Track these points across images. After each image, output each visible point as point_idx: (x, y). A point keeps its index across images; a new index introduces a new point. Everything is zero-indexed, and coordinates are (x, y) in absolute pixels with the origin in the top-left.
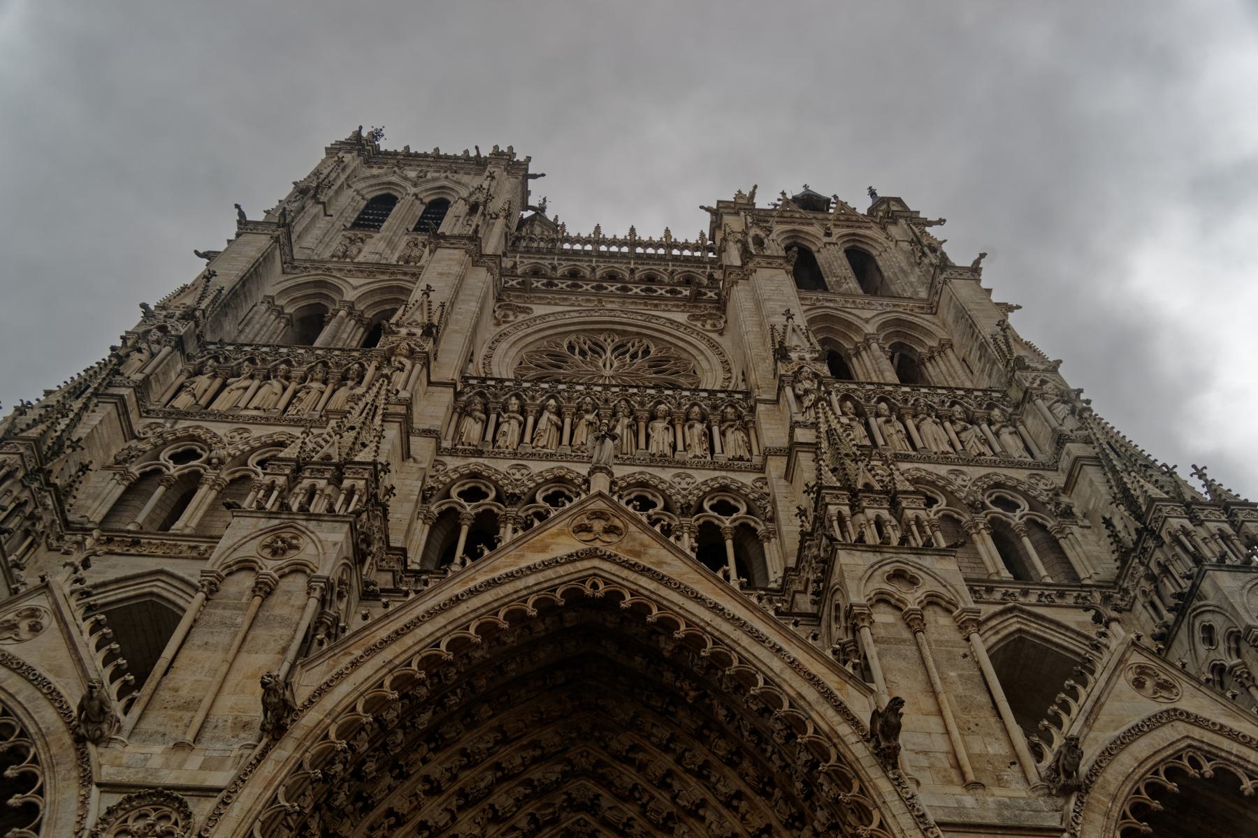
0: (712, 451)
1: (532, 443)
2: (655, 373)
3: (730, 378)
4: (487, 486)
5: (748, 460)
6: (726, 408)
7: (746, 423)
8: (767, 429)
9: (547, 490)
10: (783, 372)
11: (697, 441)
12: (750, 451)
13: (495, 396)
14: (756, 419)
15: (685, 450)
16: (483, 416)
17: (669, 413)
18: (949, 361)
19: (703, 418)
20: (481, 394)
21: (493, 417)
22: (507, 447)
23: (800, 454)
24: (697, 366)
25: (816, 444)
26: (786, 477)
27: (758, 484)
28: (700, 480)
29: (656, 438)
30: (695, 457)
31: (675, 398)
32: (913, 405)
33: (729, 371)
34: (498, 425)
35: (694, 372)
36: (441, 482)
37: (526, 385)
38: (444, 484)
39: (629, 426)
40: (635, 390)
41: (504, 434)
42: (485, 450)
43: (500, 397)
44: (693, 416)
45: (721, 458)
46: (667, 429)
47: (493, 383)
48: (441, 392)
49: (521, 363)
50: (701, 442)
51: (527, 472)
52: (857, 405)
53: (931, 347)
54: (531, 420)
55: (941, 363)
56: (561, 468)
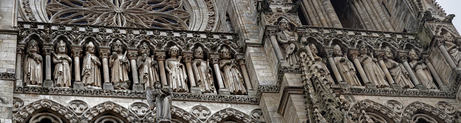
0: (217, 87)
2: (154, 9)
3: (213, 16)
5: (245, 94)
6: (222, 48)
7: (238, 61)
8: (258, 70)
10: (267, 23)
11: (205, 78)
12: (245, 85)
13: (48, 40)
14: (246, 58)
15: (197, 86)
16: (39, 56)
17: (180, 53)
19: (205, 58)
20: (34, 37)
21: (48, 57)
22: (65, 85)
24: (186, 3)
26: (279, 111)
27: (256, 115)
28: (213, 112)
29: (174, 74)
30: (207, 92)
31: (183, 40)
33: (212, 9)
34: (53, 65)
35: (183, 7)
36: (21, 116)
37: (68, 29)
38: (24, 119)
39: (153, 65)
40: (151, 33)
41: (61, 73)
43: (51, 41)
44: (197, 55)
45: (226, 91)
46: (181, 67)
47: (42, 27)
48: (8, 39)
50: (208, 79)
51: (84, 107)
54: (77, 60)
56: (109, 103)
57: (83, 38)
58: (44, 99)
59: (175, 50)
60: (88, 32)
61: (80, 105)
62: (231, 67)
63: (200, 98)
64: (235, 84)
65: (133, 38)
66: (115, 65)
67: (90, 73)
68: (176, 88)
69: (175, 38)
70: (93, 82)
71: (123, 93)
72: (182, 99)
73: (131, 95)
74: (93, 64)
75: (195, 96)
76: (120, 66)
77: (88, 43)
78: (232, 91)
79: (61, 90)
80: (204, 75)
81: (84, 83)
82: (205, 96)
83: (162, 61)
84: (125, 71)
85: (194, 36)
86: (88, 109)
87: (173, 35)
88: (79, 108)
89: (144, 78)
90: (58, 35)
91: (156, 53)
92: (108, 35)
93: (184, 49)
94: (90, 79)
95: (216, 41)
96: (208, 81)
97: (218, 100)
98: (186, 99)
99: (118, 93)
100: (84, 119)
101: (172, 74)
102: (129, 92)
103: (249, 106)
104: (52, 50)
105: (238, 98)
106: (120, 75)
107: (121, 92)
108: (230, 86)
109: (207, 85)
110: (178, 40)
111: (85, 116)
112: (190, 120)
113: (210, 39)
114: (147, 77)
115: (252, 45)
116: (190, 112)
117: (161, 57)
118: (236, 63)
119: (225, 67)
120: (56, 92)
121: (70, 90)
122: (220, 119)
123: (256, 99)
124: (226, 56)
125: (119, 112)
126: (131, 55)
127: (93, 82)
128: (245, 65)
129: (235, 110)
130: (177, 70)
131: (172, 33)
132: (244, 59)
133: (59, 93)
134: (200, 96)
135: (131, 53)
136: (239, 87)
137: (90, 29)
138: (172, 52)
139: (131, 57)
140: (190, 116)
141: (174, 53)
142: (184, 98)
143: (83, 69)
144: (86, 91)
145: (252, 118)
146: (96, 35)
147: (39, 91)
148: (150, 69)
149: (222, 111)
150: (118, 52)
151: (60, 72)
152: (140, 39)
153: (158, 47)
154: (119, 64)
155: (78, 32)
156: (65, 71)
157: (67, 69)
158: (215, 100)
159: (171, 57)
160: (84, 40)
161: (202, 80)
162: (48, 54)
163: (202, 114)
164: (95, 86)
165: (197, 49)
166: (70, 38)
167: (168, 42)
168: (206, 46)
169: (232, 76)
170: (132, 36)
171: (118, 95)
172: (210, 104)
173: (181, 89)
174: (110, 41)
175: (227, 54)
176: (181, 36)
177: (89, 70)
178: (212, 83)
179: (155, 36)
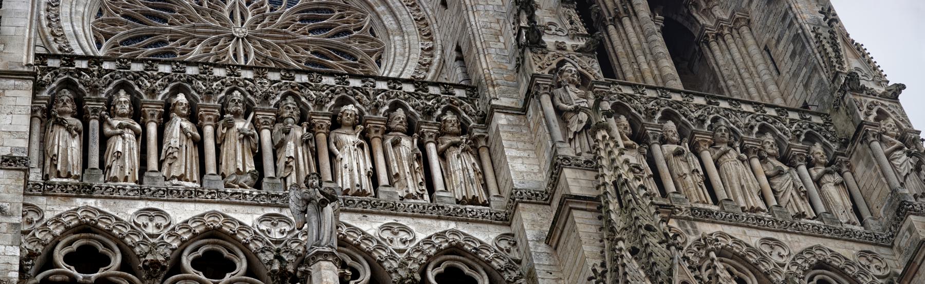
0: (431, 188)
1: (160, 168)
2: (312, 31)
3: (430, 49)
4: (106, 245)
5: (484, 204)
6: (444, 112)
7: (475, 140)
9: (196, 250)
11: (407, 169)
12: (485, 186)
13: (95, 89)
14: (491, 135)
15: (391, 184)
16: (76, 122)
17: (360, 119)
18: (745, 46)
21: (94, 124)
22: (126, 179)
23: (575, 213)
24: (376, 21)
25: (597, 199)
27: (504, 244)
28: (421, 236)
29: (346, 161)
30: (410, 196)
31: (367, 94)
32: (710, 126)
34: (104, 140)
35: (372, 31)
37: (136, 67)
39: (305, 142)
40: (305, 78)
41: (119, 155)
42: (95, 185)
43: (101, 91)
44: (395, 124)
45: (447, 197)
46: (361, 146)
49: (100, 13)
50: (413, 172)
52: (633, 121)
53: (719, 20)
54: (152, 129)
55: (733, 47)
56: (215, 214)
57: (167, 86)
58: (83, 207)
59: (350, 113)
60: (176, 75)
61: (156, 217)
62: (460, 151)
63: (396, 209)
64: (467, 184)
65: (267, 88)
66: (228, 140)
67: (176, 156)
68: (349, 186)
69: (352, 90)
70: (183, 172)
71: (243, 194)
72: (360, 209)
73: (258, 200)
74: (184, 137)
75: (385, 204)
76: (238, 142)
77: (176, 96)
78: (459, 196)
79: (119, 189)
80: (406, 164)
81: (165, 174)
82: (407, 205)
83: (324, 133)
84: (249, 152)
85: (390, 88)
86: (172, 226)
87: (348, 83)
88: (154, 224)
89: (286, 166)
90: (116, 79)
91: (313, 119)
92: (217, 81)
93: (368, 111)
94: (177, 166)
95: (432, 99)
96: (414, 175)
97: (431, 213)
98: (369, 209)
99: (232, 194)
100: (164, 245)
101: (341, 159)
102: (255, 193)
103: (491, 227)
104: (103, 109)
105: (470, 212)
106: (238, 159)
107: (240, 193)
108: (455, 188)
109: (410, 183)
110: (357, 94)
111: (166, 240)
112: (374, 250)
113: (422, 95)
114: (291, 164)
116: (375, 234)
117: (322, 125)
118: (470, 143)
119: (448, 150)
120: (108, 192)
121: (135, 188)
122: (433, 251)
123: (506, 214)
124: (451, 128)
125: (234, 231)
126: (262, 121)
127: (183, 172)
128: (489, 149)
129: (464, 234)
130: (352, 152)
131: (346, 80)
132: (487, 135)
133: (114, 195)
134: (396, 204)
135: (261, 116)
136: (474, 191)
137: (181, 68)
138: (345, 117)
139: (262, 123)
140: (375, 244)
141: (348, 118)
143: (164, 147)
144: (169, 191)
145: (496, 251)
146: (192, 80)
147: (74, 190)
148: (300, 149)
149: (438, 235)
150: (236, 114)
151: (118, 152)
152: (281, 90)
153: (317, 107)
154: (238, 138)
155: (155, 73)
156: (127, 150)
157: (132, 146)
158: (425, 213)
159: (343, 127)
160: (167, 90)
161: (401, 174)
163: (399, 239)
164: (187, 180)
165: (395, 113)
166: (140, 86)
167: (336, 97)
168: (413, 108)
169: (461, 168)
170: (265, 83)
171: (233, 200)
172: (416, 220)
173: (358, 190)
174: (220, 93)
175: (453, 125)
176: (365, 86)
177: (176, 150)
178: (421, 181)
179: (311, 85)
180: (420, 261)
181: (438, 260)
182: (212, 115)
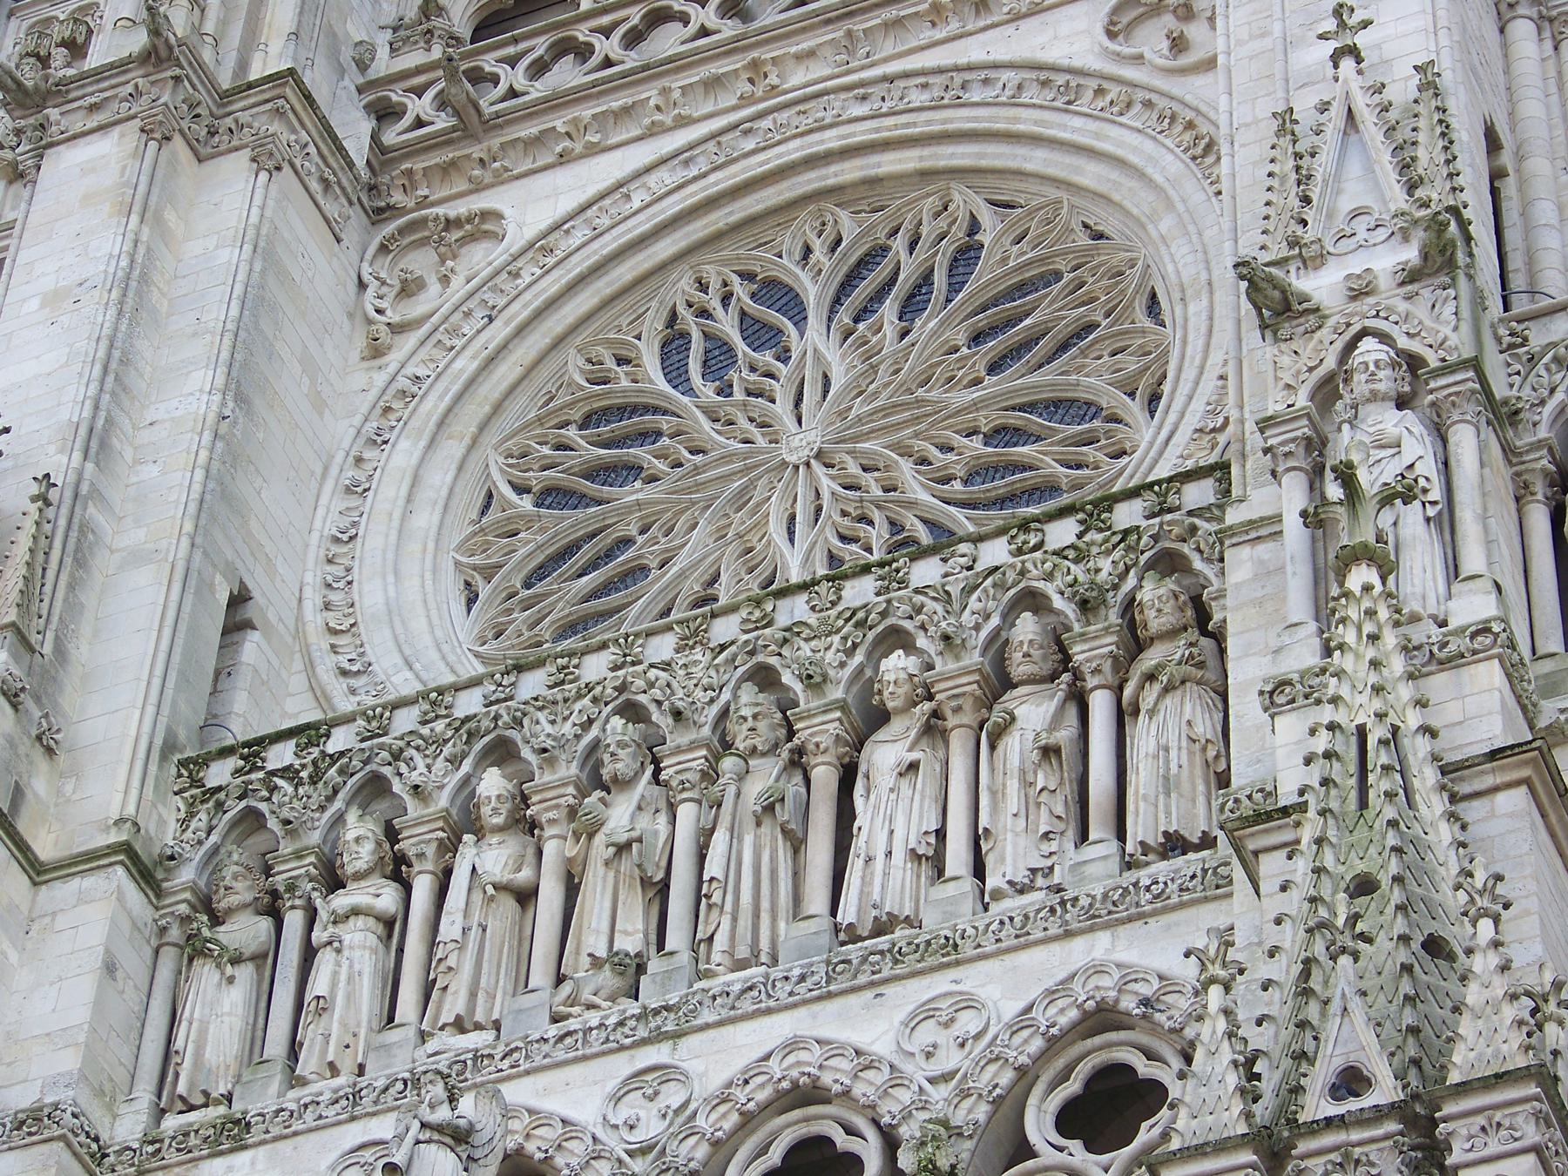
63: (956, 946)
72: (863, 979)
75: (928, 943)
97: (1045, 929)
98: (886, 973)
99: (561, 1039)
105: (1148, 889)
110: (919, 610)
115: (1253, 535)
142: (874, 973)
151: (318, 998)
157: (357, 967)
162: (288, 904)
170: (696, 663)
177: (452, 946)
180: (990, 1092)
181: (1060, 1063)
182: (557, 806)
